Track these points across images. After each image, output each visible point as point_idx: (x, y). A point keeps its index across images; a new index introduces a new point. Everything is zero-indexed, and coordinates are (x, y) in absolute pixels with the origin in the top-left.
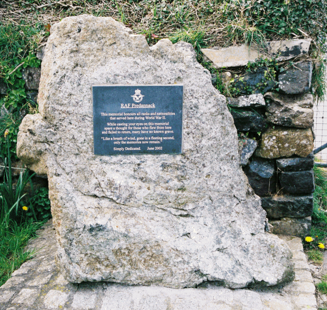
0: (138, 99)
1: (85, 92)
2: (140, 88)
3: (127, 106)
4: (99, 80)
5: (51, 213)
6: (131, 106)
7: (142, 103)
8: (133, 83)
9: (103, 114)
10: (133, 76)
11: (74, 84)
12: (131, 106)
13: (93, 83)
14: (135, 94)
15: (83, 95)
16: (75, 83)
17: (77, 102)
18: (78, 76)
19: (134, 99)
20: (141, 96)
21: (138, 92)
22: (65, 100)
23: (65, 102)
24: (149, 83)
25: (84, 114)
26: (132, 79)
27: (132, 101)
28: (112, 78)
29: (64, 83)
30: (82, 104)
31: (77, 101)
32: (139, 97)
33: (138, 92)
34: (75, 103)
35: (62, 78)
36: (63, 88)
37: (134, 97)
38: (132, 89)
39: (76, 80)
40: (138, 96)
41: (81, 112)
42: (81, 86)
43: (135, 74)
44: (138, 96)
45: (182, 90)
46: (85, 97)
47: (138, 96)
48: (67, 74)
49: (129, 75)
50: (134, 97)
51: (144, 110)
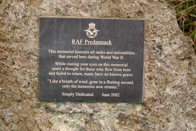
0: (92, 34)
1: (31, 24)
2: (94, 21)
3: (79, 42)
4: (48, 11)
5: (54, 18)
6: (84, 42)
7: (98, 38)
8: (86, 15)
9: (51, 51)
10: (88, 8)
11: (18, 15)
12: (84, 42)
13: (40, 14)
14: (89, 29)
15: (29, 28)
16: (20, 14)
17: (21, 37)
18: (24, 7)
19: (87, 34)
20: (96, 31)
21: (92, 25)
22: (8, 34)
23: (8, 37)
24: (105, 17)
25: (29, 51)
26: (86, 11)
27: (84, 36)
28: (62, 9)
29: (8, 14)
30: (27, 39)
31: (21, 35)
32: (94, 31)
33: (92, 25)
34: (19, 38)
35: (6, 9)
36: (6, 20)
37: (88, 31)
38: (85, 23)
39: (22, 11)
40: (92, 30)
41: (25, 49)
42: (26, 18)
43: (89, 6)
44: (92, 30)
45: (144, 25)
46: (31, 31)
47: (92, 30)
48: (11, 5)
49: (83, 6)
50: (88, 31)
51: (100, 48)
